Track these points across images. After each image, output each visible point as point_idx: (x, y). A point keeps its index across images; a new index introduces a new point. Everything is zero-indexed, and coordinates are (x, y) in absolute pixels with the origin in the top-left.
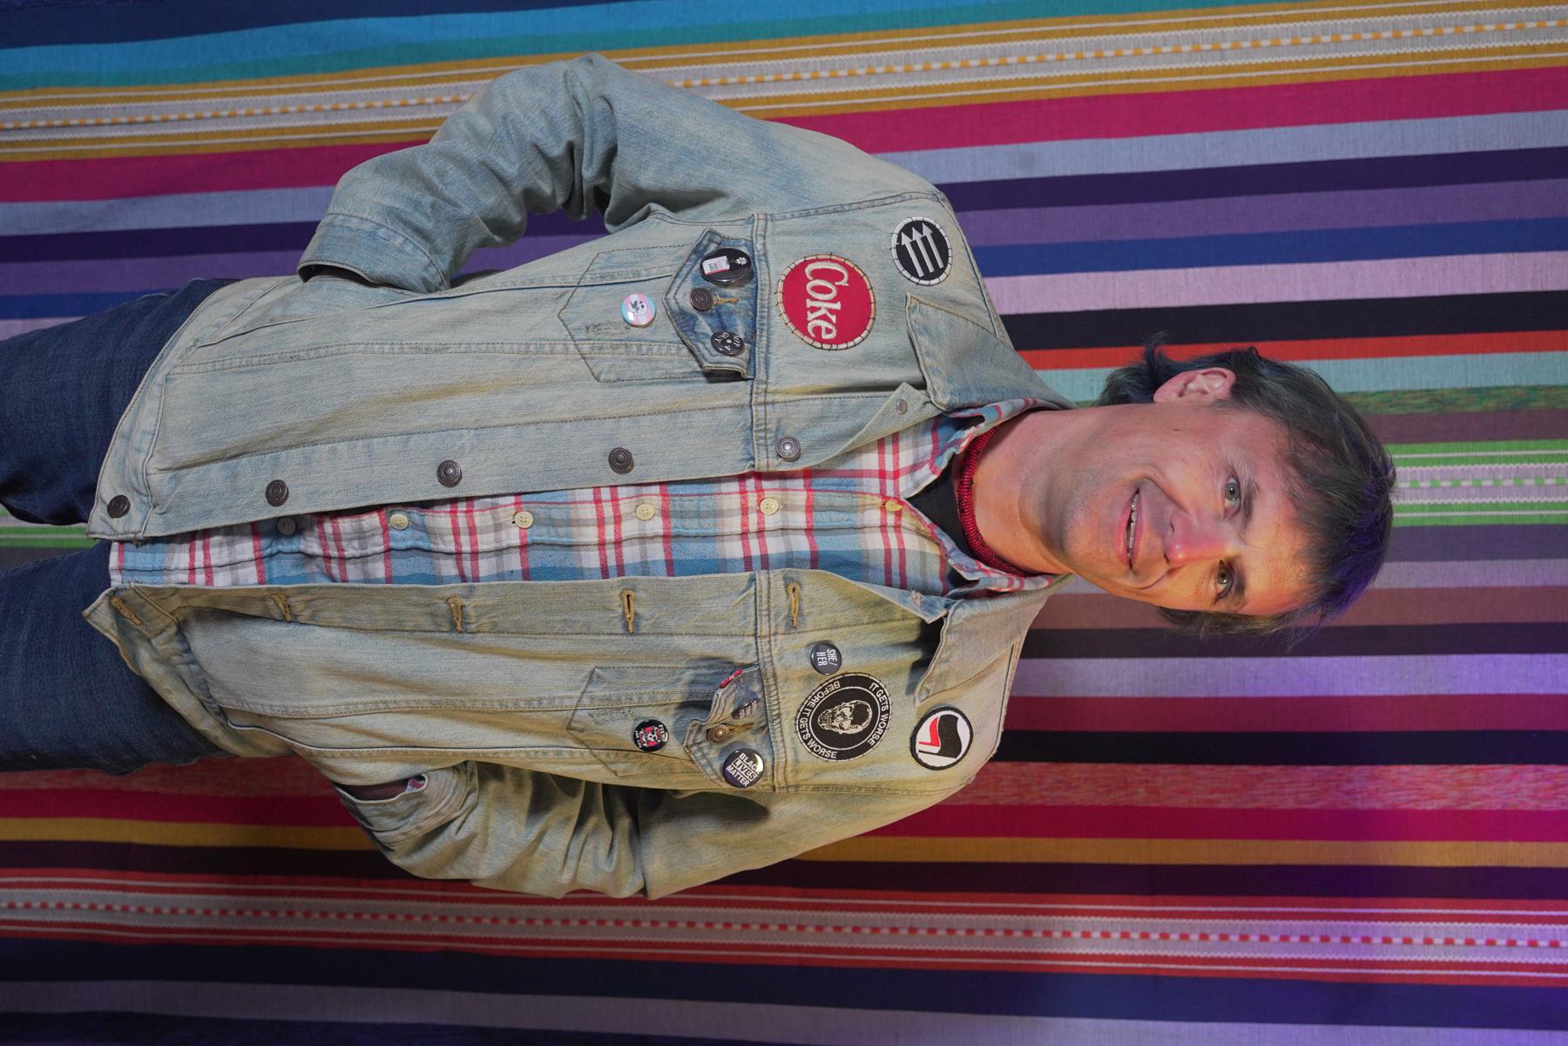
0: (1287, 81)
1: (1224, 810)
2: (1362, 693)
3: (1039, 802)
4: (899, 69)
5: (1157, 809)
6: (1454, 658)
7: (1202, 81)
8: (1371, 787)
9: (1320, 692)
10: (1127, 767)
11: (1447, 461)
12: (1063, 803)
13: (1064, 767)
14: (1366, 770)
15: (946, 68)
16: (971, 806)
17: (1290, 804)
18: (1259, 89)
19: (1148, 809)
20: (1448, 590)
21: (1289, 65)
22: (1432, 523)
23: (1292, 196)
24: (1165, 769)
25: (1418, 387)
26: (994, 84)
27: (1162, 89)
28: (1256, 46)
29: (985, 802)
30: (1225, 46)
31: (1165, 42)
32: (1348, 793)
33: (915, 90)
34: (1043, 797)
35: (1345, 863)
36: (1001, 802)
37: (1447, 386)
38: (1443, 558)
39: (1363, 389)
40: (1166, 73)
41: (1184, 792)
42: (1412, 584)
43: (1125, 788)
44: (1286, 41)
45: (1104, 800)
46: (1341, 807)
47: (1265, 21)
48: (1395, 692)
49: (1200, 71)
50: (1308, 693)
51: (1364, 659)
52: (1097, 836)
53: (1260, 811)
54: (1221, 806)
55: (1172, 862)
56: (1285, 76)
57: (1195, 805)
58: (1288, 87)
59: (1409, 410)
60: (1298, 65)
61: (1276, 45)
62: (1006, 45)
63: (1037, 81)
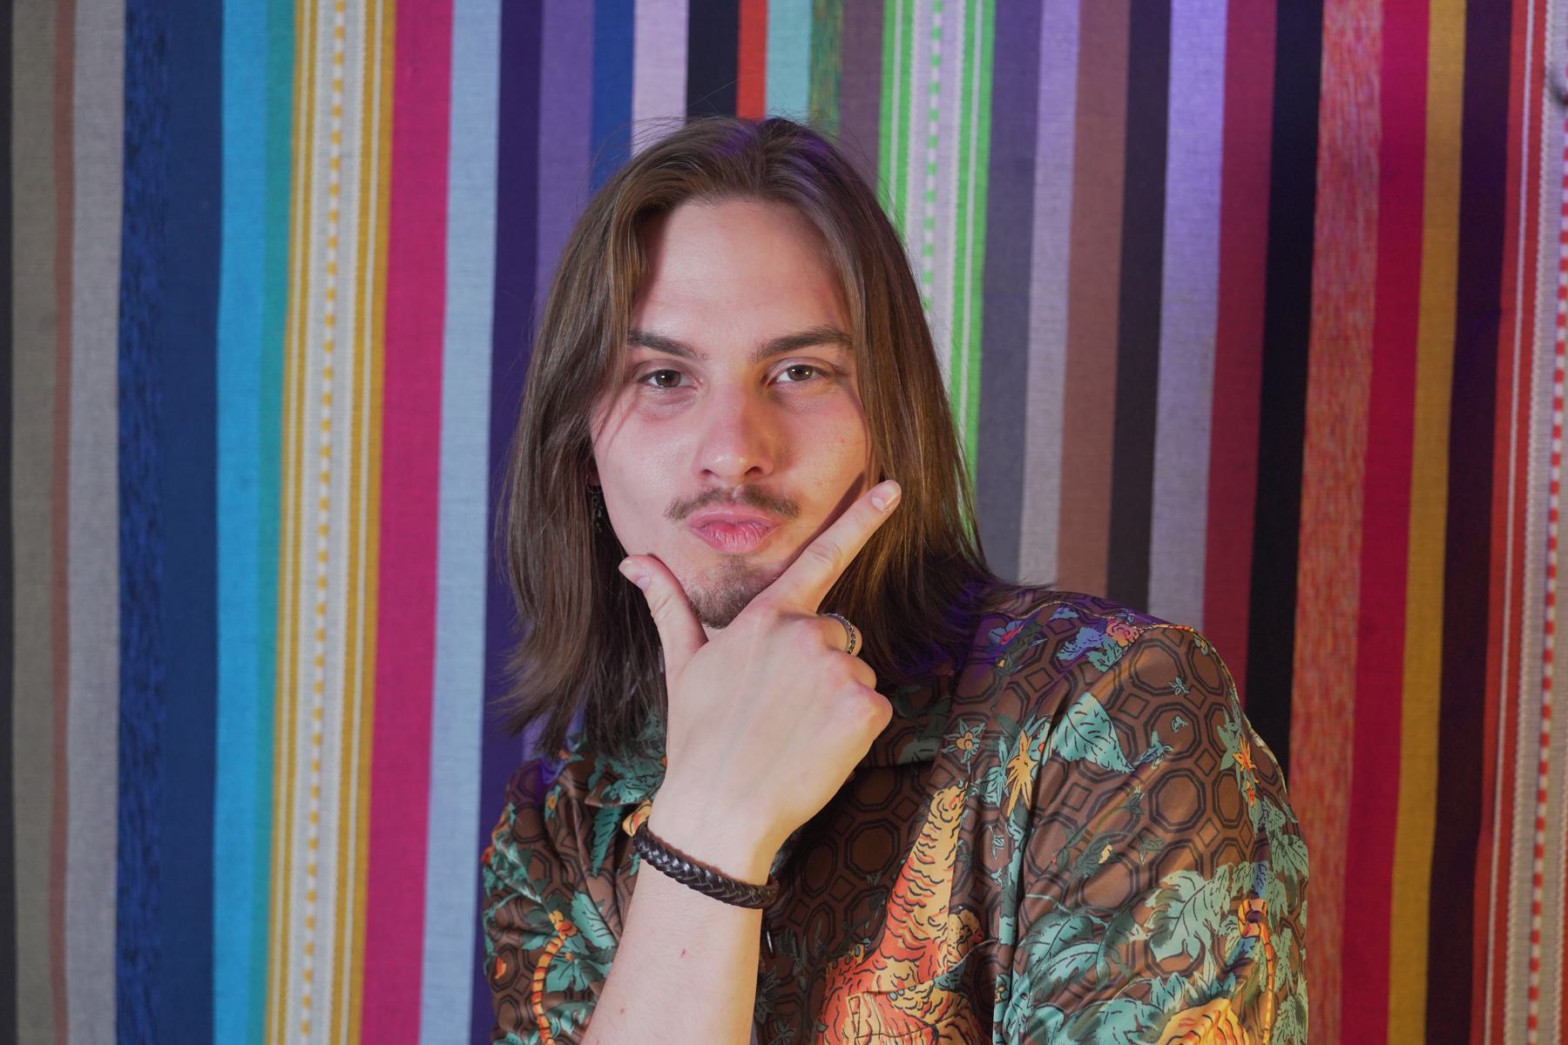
0: (390, 73)
3: (1361, 463)
4: (321, 596)
5: (1379, 298)
7: (379, 185)
9: (1219, 66)
12: (1364, 428)
13: (1311, 423)
15: (326, 530)
19: (1379, 310)
21: (368, 69)
24: (1318, 283)
26: (356, 465)
27: (385, 238)
28: (339, 111)
29: (1358, 539)
30: (335, 151)
31: (323, 231)
33: (352, 576)
34: (1354, 456)
36: (1359, 515)
40: (363, 231)
41: (1353, 258)
43: (1347, 339)
44: (338, 72)
45: (1365, 371)
49: (365, 188)
54: (1375, 207)
56: (382, 76)
57: (1373, 243)
60: (369, 57)
61: (340, 85)
62: (307, 445)
63: (357, 407)
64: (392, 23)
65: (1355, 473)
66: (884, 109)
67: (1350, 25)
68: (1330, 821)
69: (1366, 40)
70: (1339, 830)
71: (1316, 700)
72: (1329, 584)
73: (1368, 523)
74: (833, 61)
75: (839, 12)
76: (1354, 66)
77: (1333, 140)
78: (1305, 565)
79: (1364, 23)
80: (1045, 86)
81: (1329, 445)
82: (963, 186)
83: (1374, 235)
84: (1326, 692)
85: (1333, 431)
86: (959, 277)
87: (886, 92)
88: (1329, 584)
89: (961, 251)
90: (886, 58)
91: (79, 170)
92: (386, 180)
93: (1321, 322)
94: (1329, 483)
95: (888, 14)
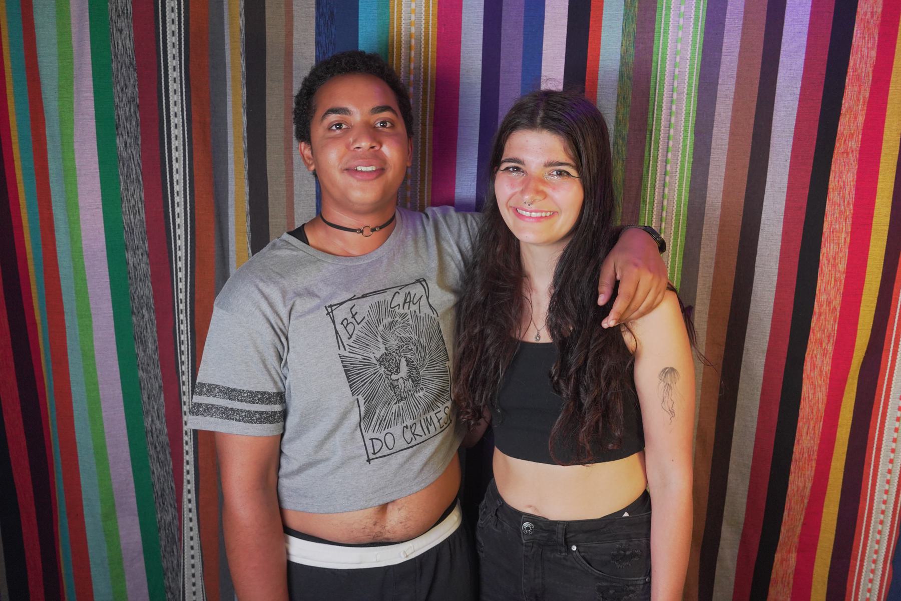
1: (871, 94)
3: (851, 207)
23: (503, 32)
29: (848, 240)
43: (848, 154)
45: (854, 167)
52: (878, 172)
58: (439, 28)
65: (849, 211)
66: (655, 49)
72: (835, 259)
74: (633, 27)
75: (637, 5)
78: (824, 250)
80: (725, 40)
82: (690, 85)
84: (829, 303)
86: (686, 126)
87: (656, 42)
88: (835, 259)
89: (688, 114)
95: (659, 6)
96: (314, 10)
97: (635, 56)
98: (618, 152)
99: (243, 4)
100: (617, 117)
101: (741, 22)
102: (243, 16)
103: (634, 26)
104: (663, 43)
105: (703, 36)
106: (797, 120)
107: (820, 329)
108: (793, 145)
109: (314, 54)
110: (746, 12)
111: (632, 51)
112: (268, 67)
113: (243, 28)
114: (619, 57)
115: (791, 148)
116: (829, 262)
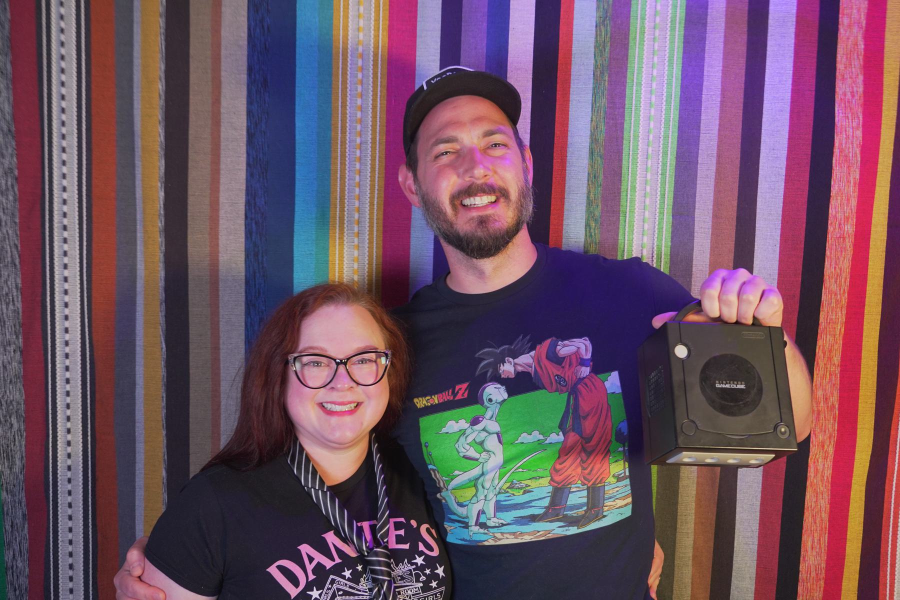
2: (790, 81)
6: (770, 22)
8: (849, 81)
10: (829, 236)
11: (643, 19)
13: (826, 278)
14: (839, 83)
16: (844, 339)
17: (859, 133)
18: (388, 122)
20: (726, 23)
21: (374, 100)
22: (682, 29)
24: (832, 211)
25: (594, 32)
29: (843, 330)
30: (358, 140)
32: (853, 96)
35: (896, 102)
37: (595, 14)
38: (705, 25)
39: (592, 68)
40: (373, 180)
41: (848, 200)
42: (721, 46)
46: (862, 101)
47: (344, 114)
48: (792, 59)
49: (373, 159)
50: (787, 116)
51: (766, 79)
53: (862, 152)
55: (887, 211)
57: (856, 194)
59: (608, 39)
61: (361, 108)
64: (386, 77)
65: (844, 302)
66: (626, 126)
67: (848, 90)
68: (825, 458)
69: (857, 97)
70: (829, 463)
71: (822, 404)
72: (830, 351)
73: (847, 323)
74: (603, 102)
76: (851, 109)
77: (841, 144)
78: (820, 343)
79: (855, 89)
80: (703, 117)
81: (834, 287)
82: (664, 165)
83: (857, 190)
85: (836, 282)
87: (626, 118)
90: (627, 102)
91: (223, 144)
92: (383, 156)
93: (832, 230)
94: (833, 305)
95: (628, 81)
96: (245, 76)
97: (606, 133)
98: (591, 236)
99: (163, 67)
100: (588, 197)
101: (719, 99)
102: (163, 80)
103: (605, 100)
104: (635, 121)
105: (677, 113)
106: (784, 203)
107: (821, 430)
108: (782, 229)
109: (245, 124)
110: (723, 90)
111: (603, 127)
112: (191, 137)
113: (162, 94)
114: (589, 133)
115: (779, 232)
116: (824, 354)
